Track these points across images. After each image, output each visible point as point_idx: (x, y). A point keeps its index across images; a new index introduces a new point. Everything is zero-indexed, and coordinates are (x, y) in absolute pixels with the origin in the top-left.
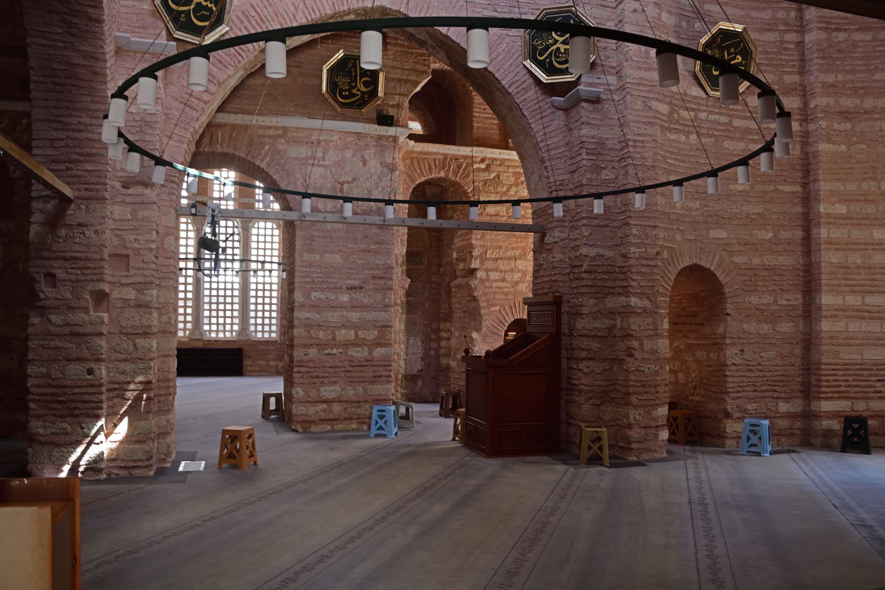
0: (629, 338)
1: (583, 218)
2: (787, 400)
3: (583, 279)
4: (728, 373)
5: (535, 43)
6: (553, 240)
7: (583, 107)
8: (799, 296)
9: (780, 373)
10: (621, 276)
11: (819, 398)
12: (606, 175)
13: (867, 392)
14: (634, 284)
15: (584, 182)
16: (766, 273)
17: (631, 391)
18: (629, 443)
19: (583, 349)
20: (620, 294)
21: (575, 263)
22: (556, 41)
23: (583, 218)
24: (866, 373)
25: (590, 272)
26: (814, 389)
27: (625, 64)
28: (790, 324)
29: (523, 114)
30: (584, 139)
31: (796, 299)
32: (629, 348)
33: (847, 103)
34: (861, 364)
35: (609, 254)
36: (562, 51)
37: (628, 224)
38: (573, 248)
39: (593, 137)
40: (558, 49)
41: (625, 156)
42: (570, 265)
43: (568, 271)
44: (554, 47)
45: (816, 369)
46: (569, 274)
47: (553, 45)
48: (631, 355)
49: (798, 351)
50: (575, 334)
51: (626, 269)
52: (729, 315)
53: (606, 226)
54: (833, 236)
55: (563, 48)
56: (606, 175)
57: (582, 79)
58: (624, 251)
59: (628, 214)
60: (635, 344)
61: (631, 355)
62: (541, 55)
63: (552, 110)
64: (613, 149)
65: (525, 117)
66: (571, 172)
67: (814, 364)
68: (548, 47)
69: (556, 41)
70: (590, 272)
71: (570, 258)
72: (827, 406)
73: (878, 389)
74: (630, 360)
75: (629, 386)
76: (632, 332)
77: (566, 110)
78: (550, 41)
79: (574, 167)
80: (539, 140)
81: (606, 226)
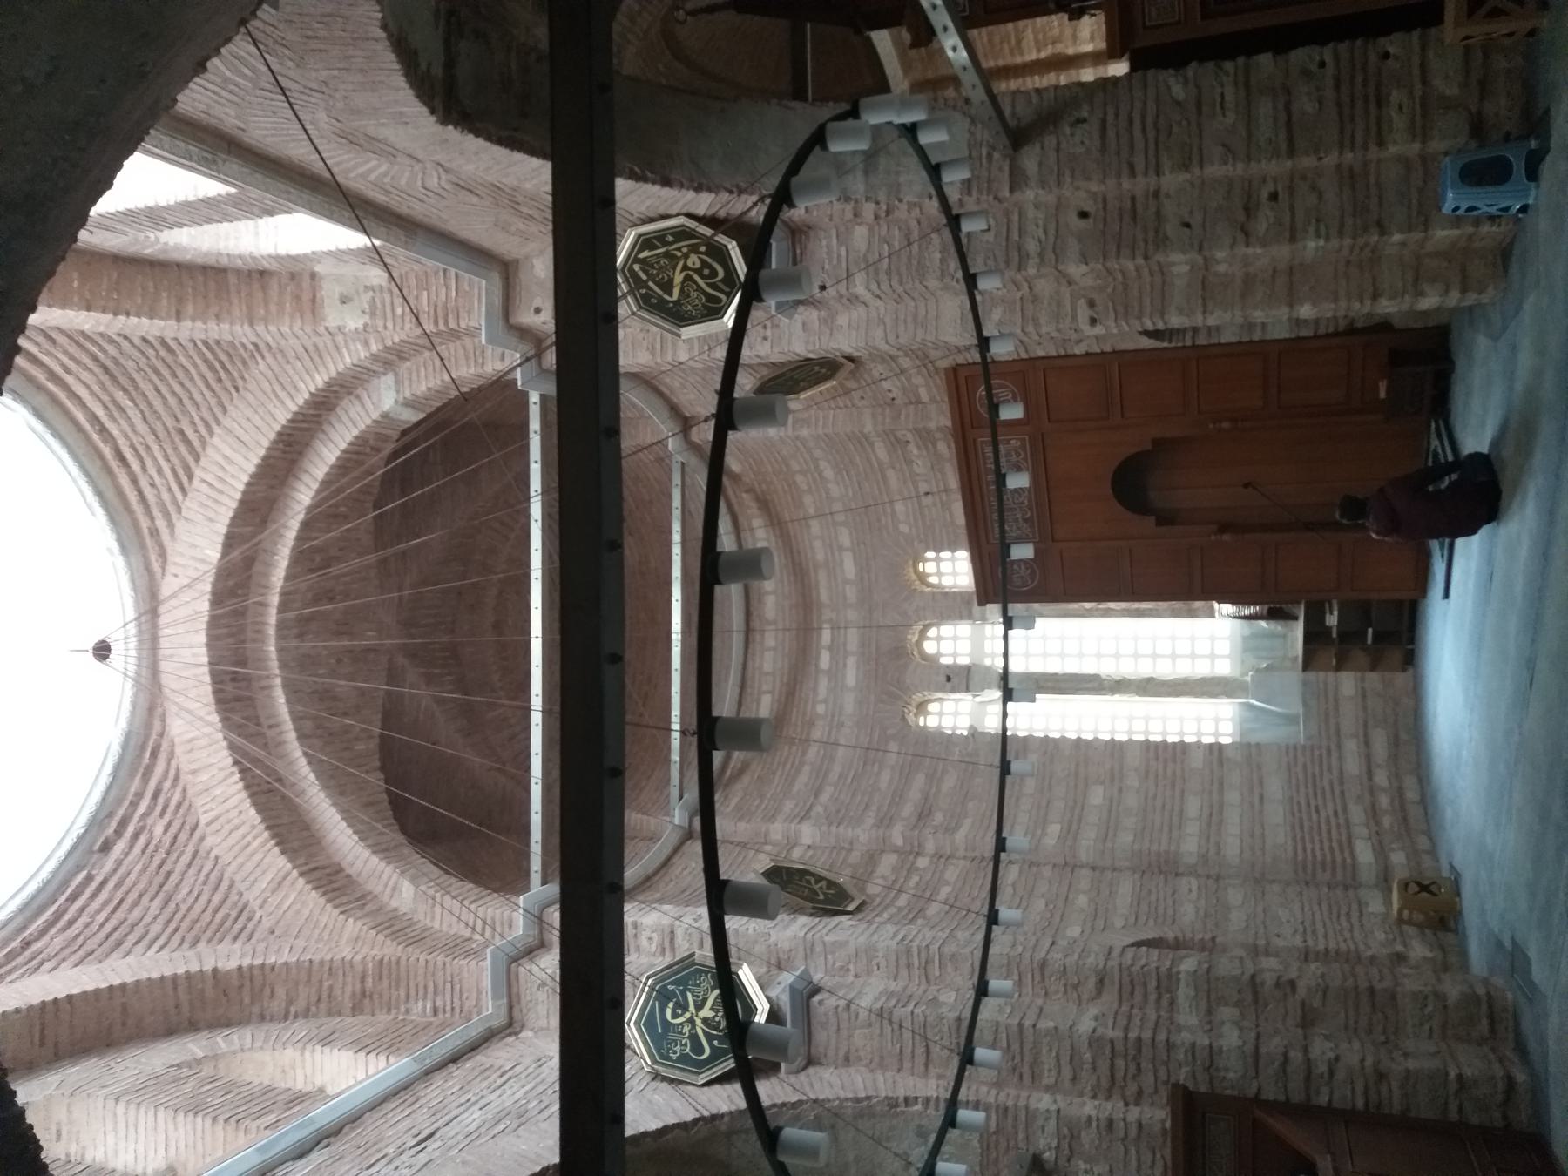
0: (1258, 980)
1: (1021, 1025)
2: (1361, 905)
3: (1139, 1039)
4: (1321, 947)
5: (675, 1057)
6: (1053, 1122)
7: (820, 1002)
8: (1184, 880)
9: (1316, 908)
10: (1138, 997)
11: (1354, 866)
12: (948, 997)
13: (1338, 825)
14: (1153, 966)
15: (953, 1015)
16: (1144, 907)
17: (1366, 985)
18: (1476, 999)
19: (1285, 1055)
20: (1172, 1002)
21: (1104, 1067)
22: (691, 1021)
23: (1021, 1025)
24: (1306, 824)
25: (1127, 1029)
26: (1339, 876)
27: (773, 938)
28: (1231, 891)
29: (794, 1105)
30: (878, 1006)
31: (1188, 885)
32: (1278, 985)
33: (908, 810)
34: (1293, 828)
35: (1094, 1010)
36: (711, 1014)
37: (1043, 964)
38: (1074, 1079)
39: (877, 999)
40: (705, 1021)
41: (923, 954)
42: (1108, 1098)
43: (1121, 1104)
44: (699, 1022)
45: (1304, 868)
46: (1127, 1104)
47: (694, 1025)
48: (1292, 984)
49: (1276, 888)
50: (1255, 1084)
51: (1126, 980)
52: (1213, 939)
53: (1041, 1009)
54: (1093, 835)
55: (706, 1012)
56: (948, 997)
57: (773, 994)
58: (1091, 983)
59: (1026, 961)
60: (1269, 979)
61: (1292, 984)
62: (702, 1052)
63: (802, 1076)
64: (905, 989)
65: (800, 1102)
66: (926, 1065)
67: (1296, 872)
68: (694, 1038)
69: (691, 1021)
70: (1127, 1029)
71: (1094, 1097)
72: (1365, 854)
73: (1331, 813)
74: (1302, 991)
75: (1356, 988)
76: (1247, 976)
77: (811, 1062)
78: (686, 1029)
79: (920, 1050)
80: (850, 1095)
81: (1041, 1009)
